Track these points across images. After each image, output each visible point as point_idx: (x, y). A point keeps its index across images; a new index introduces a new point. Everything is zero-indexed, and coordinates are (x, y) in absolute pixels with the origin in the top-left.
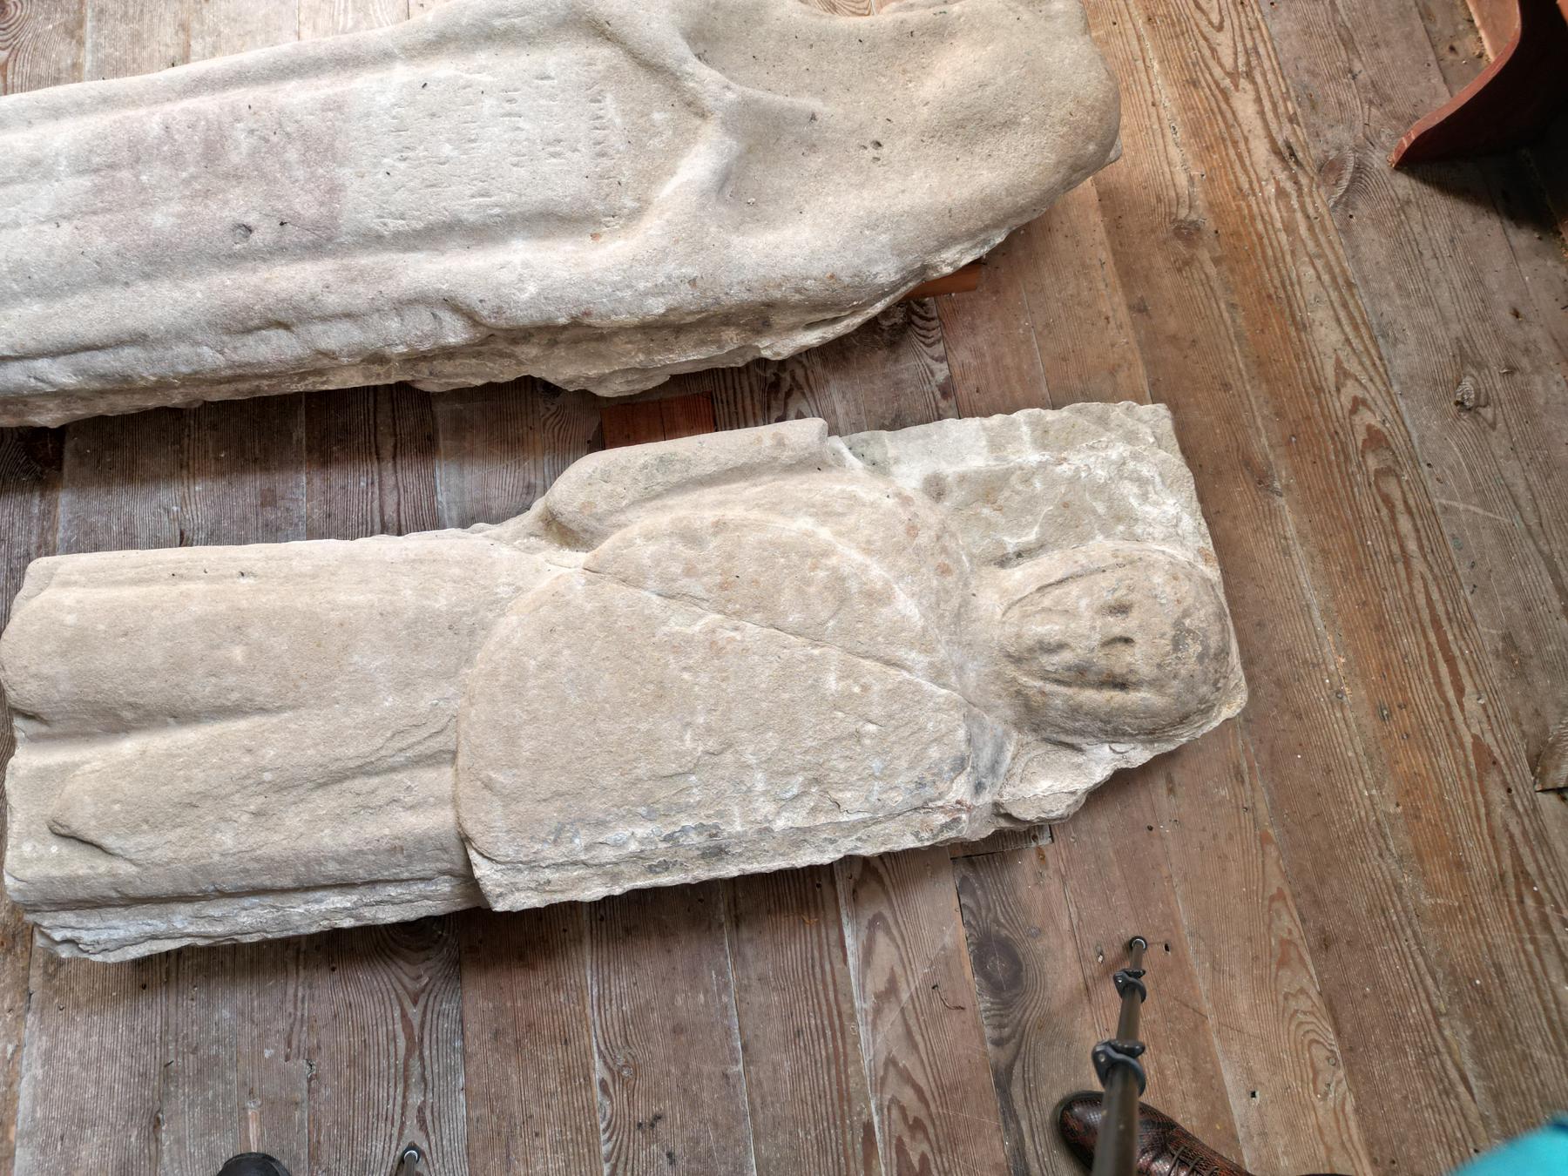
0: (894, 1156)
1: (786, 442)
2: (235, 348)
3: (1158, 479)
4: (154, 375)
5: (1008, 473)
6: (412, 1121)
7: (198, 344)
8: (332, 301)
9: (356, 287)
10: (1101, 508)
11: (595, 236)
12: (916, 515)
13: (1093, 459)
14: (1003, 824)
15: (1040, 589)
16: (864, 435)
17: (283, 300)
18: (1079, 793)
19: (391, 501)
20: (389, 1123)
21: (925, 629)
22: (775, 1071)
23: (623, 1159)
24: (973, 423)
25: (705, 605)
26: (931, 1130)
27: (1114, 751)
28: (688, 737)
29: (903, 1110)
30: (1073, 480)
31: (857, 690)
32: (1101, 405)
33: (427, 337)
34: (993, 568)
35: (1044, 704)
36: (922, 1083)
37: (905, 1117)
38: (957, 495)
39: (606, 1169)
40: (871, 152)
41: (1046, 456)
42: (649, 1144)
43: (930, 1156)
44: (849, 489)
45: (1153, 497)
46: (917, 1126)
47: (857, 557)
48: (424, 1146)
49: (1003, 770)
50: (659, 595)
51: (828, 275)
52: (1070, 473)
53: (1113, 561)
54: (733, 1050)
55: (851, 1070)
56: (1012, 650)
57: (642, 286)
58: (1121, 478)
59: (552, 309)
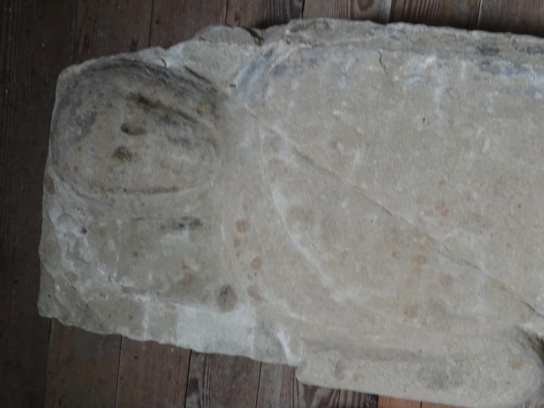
1: (334, 370)
3: (63, 255)
5: (168, 294)
10: (112, 245)
12: (249, 277)
13: (104, 285)
14: (259, 32)
15: (175, 189)
16: (268, 360)
18: (198, 38)
21: (273, 180)
25: (442, 248)
27: (163, 61)
28: (487, 144)
30: (124, 272)
31: (340, 146)
32: (84, 327)
34: (204, 221)
35: (201, 104)
41: (137, 297)
45: (72, 244)
47: (305, 252)
49: (247, 67)
50: (477, 268)
52: (124, 278)
53: (115, 197)
56: (212, 148)
58: (88, 264)
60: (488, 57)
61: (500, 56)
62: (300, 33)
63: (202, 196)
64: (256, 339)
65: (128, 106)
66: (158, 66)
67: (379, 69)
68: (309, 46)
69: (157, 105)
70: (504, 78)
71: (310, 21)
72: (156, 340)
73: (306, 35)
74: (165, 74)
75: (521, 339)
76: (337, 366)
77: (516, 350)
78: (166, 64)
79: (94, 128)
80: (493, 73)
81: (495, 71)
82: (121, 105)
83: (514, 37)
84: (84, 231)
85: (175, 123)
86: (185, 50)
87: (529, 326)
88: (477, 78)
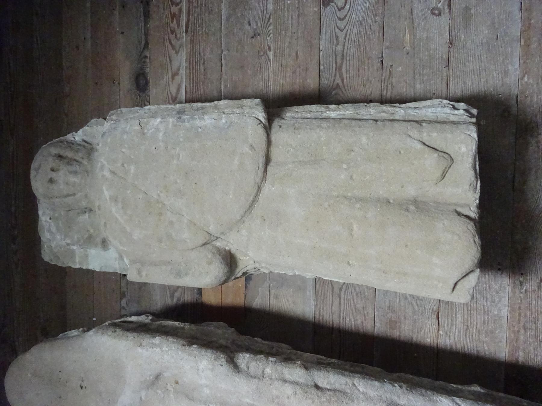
0: (181, 23)
2: (346, 385)
3: (45, 230)
4: (394, 386)
6: (341, 39)
7: (363, 393)
8: (288, 390)
9: (277, 394)
11: (177, 383)
15: (74, 194)
17: (310, 399)
19: (335, 308)
20: (350, 40)
22: (212, 52)
23: (265, 24)
24: (91, 268)
26: (169, 30)
29: (176, 37)
31: (125, 165)
33: (256, 361)
36: (169, 46)
37: (176, 35)
38: (99, 240)
39: (271, 20)
40: (84, 385)
42: (256, 29)
43: (170, 22)
44: (122, 248)
46: (173, 32)
48: (337, 30)
50: (183, 216)
51: (103, 335)
54: (224, 60)
55: (189, 50)
56: (86, 174)
57: (158, 349)
59: (195, 352)
60: (181, 115)
61: (185, 114)
62: (112, 117)
63: (86, 196)
64: (119, 263)
65: (53, 159)
66: (72, 141)
67: (139, 128)
68: (115, 122)
69: (66, 158)
70: (186, 124)
71: (115, 111)
72: (81, 267)
73: (114, 117)
74: (73, 144)
75: (213, 251)
76: (139, 271)
77: (210, 256)
78: (75, 139)
79: (40, 171)
80: (182, 122)
81: (183, 121)
82: (50, 159)
83: (193, 104)
84: (50, 219)
85: (71, 165)
86: (83, 131)
87: (218, 244)
88: (175, 126)
